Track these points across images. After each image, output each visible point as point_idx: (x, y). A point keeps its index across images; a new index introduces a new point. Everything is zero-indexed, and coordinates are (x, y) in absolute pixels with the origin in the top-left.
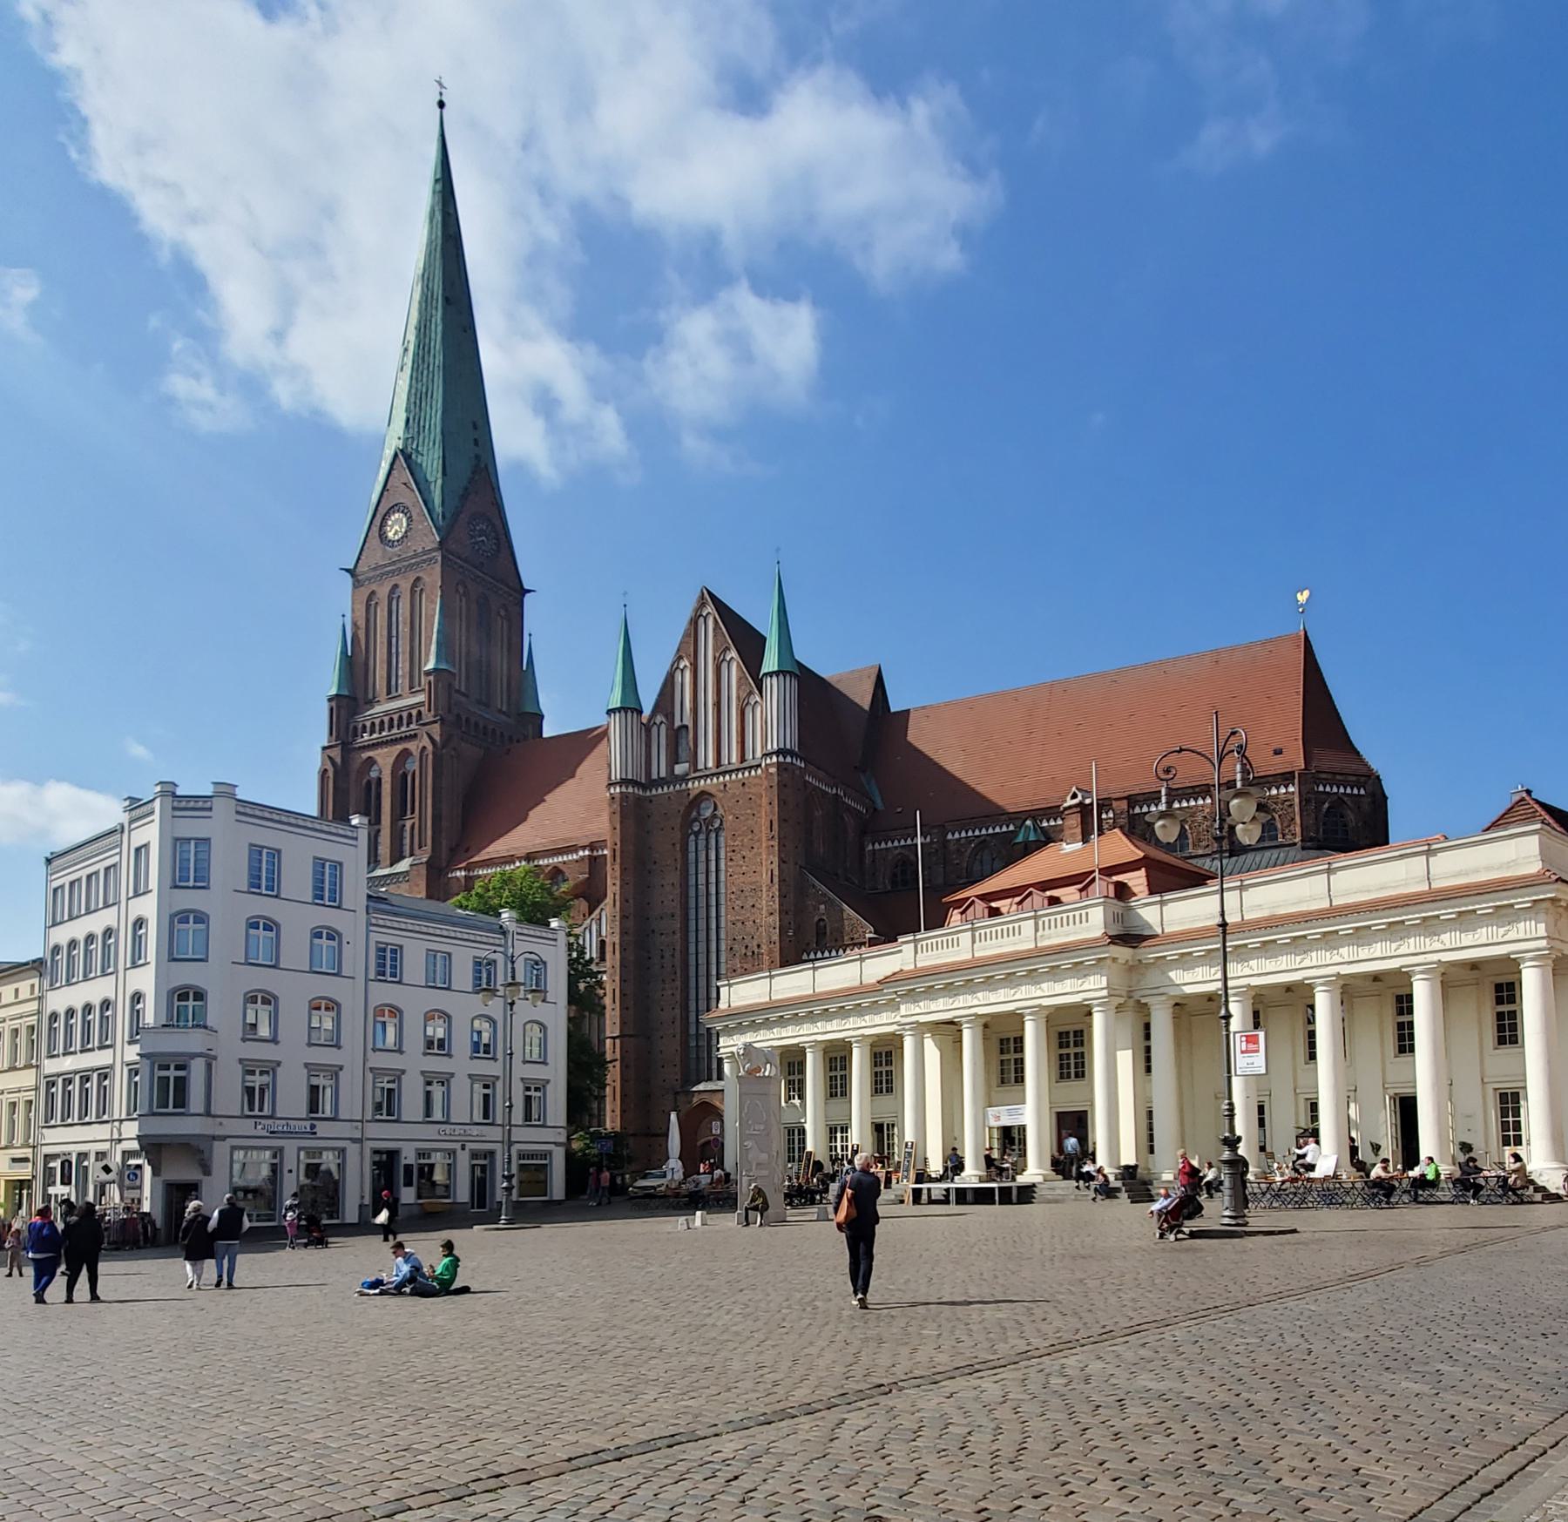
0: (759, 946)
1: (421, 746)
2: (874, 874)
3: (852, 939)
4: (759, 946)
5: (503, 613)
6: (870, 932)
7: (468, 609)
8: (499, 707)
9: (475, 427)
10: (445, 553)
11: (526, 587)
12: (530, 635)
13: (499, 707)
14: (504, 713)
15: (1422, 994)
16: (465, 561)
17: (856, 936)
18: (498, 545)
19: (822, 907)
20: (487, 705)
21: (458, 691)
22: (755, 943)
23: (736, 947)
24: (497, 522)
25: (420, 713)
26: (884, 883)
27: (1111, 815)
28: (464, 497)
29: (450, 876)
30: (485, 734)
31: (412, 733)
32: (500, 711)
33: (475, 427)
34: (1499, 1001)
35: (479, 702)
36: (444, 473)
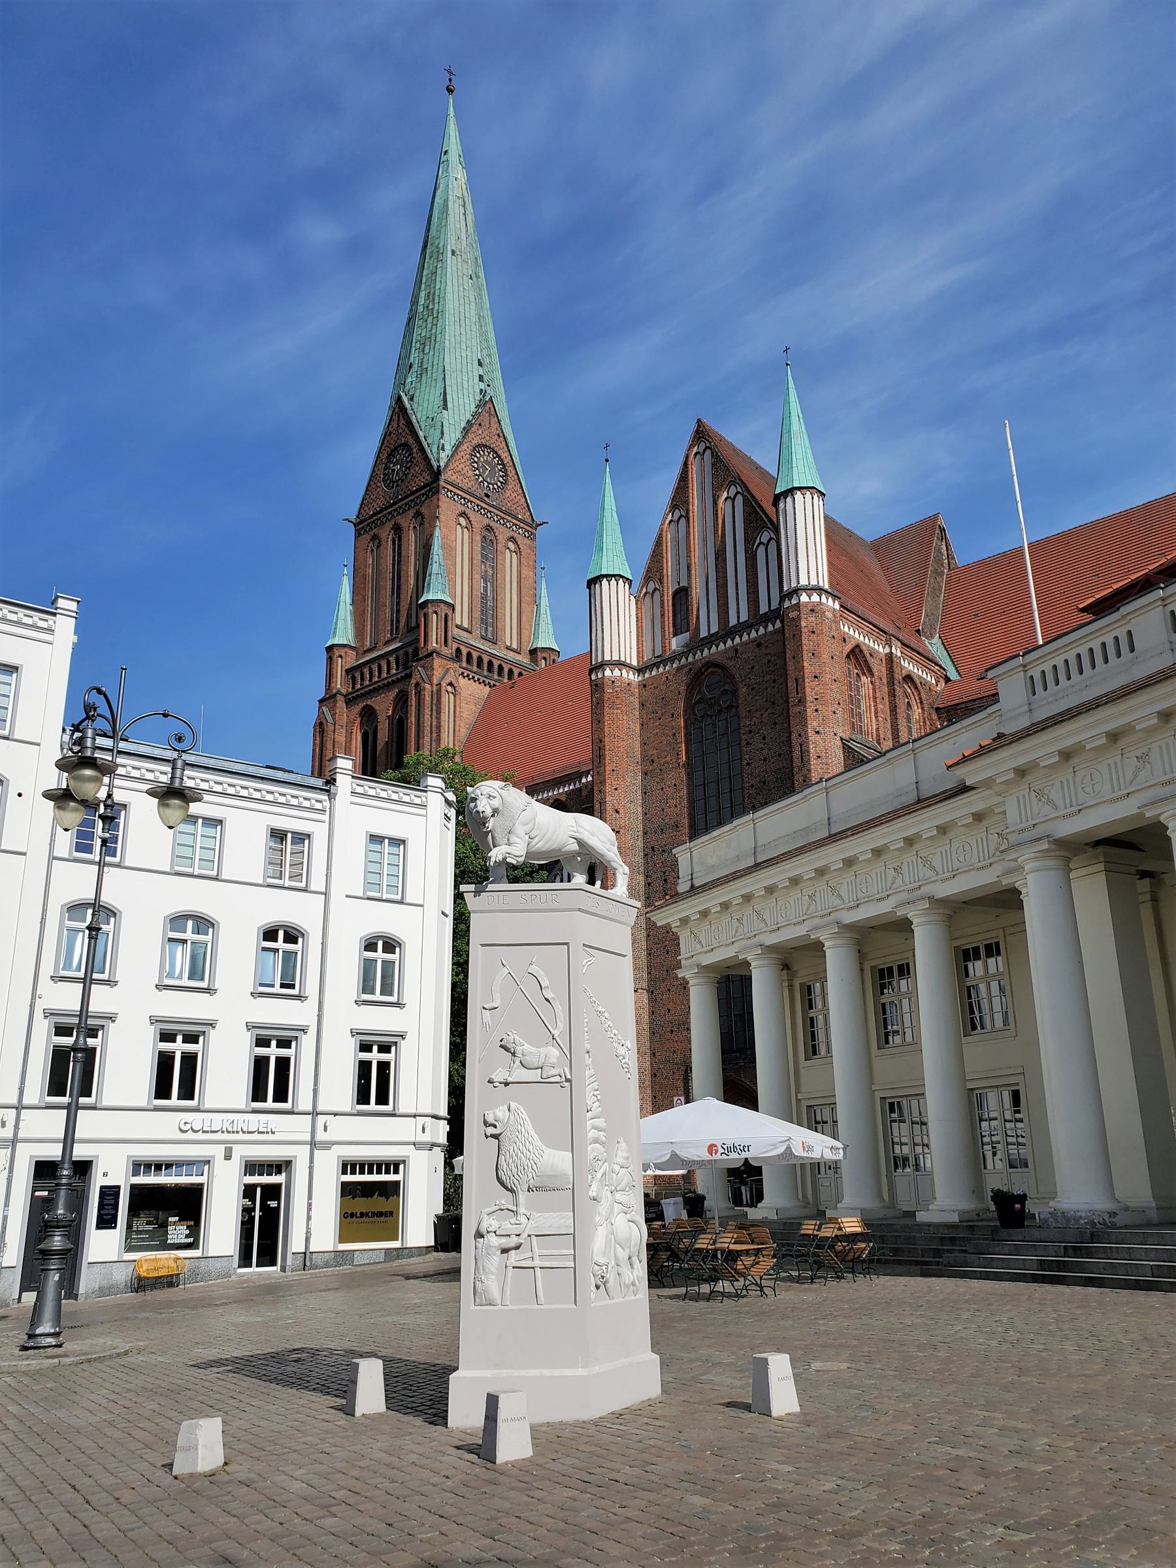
28: (466, 431)
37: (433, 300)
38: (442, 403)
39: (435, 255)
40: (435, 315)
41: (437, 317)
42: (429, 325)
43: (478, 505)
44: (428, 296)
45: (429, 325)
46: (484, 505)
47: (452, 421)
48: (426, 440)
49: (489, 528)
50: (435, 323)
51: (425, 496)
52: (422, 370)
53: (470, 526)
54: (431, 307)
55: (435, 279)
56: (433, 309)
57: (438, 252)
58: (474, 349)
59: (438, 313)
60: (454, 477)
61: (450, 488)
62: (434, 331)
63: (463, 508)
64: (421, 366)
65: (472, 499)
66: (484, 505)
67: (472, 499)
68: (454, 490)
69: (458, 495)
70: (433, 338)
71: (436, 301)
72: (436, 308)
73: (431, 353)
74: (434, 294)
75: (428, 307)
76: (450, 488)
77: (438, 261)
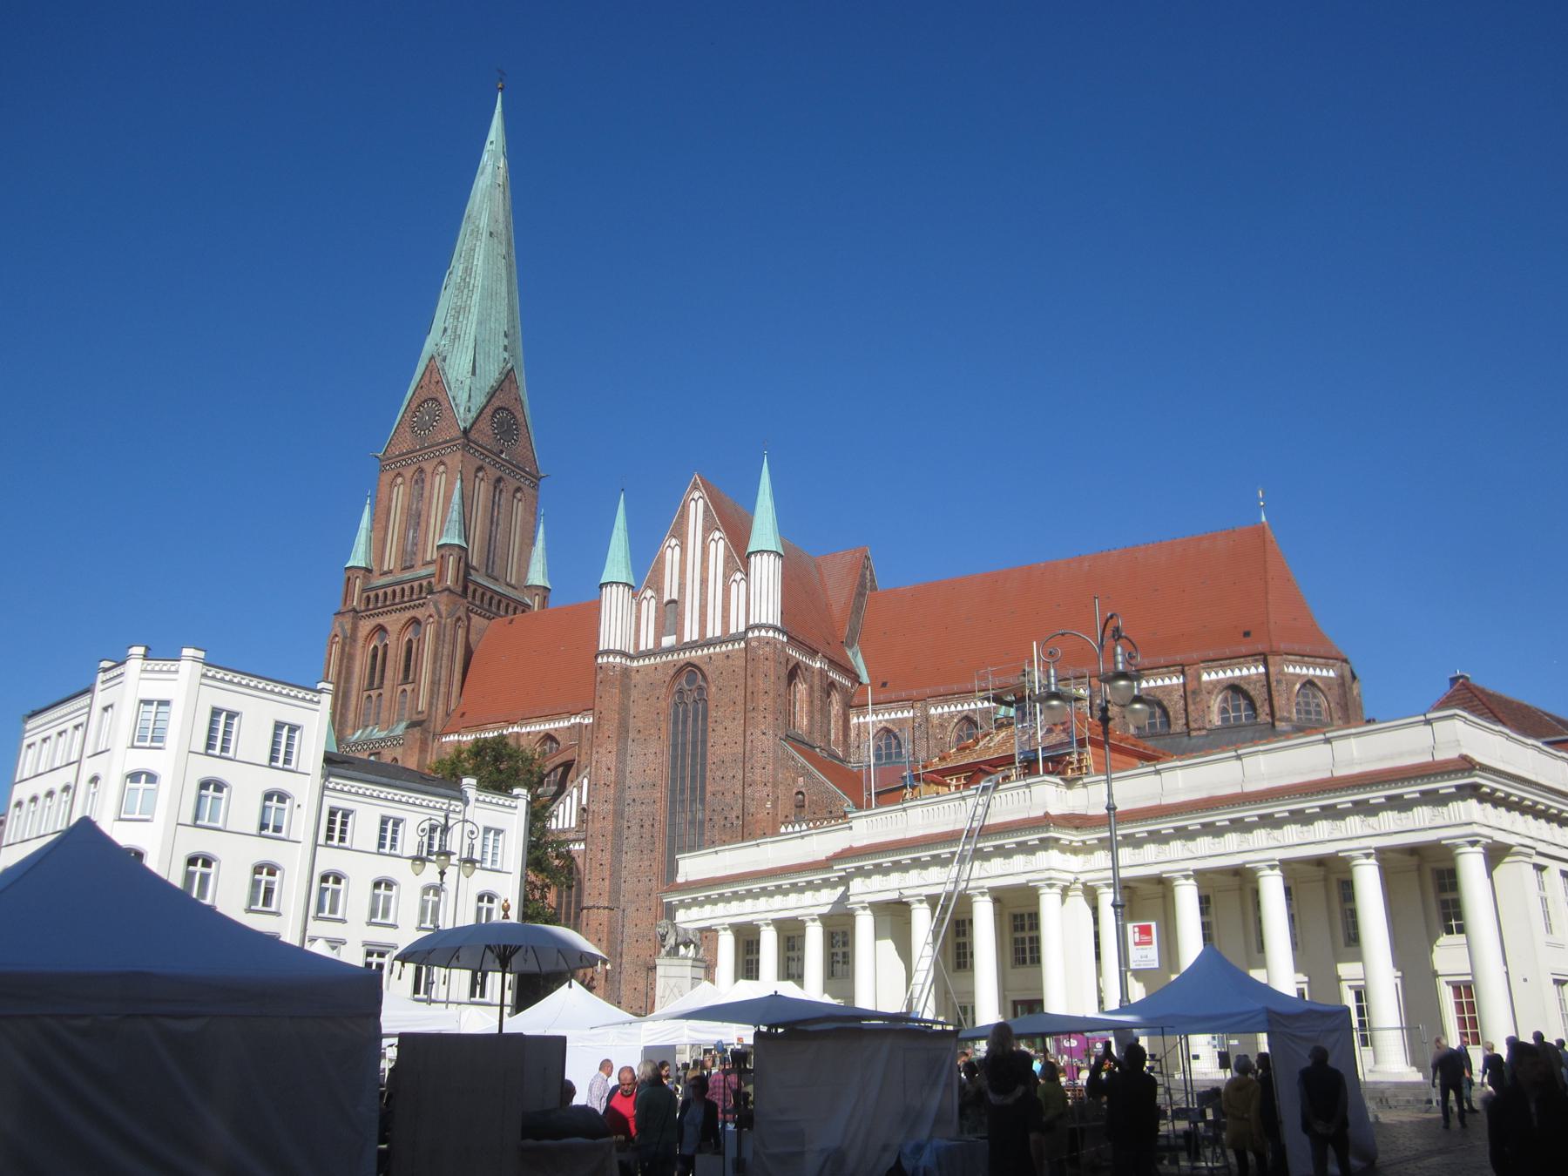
29: (444, 740)
36: (474, 373)
37: (471, 274)
38: (471, 369)
39: (475, 234)
40: (471, 288)
41: (473, 290)
42: (465, 297)
44: (466, 270)
45: (465, 297)
47: (478, 386)
48: (454, 400)
50: (470, 295)
52: (456, 335)
54: (467, 280)
55: (474, 256)
56: (469, 283)
57: (478, 231)
59: (474, 286)
62: (468, 302)
64: (455, 332)
70: (467, 309)
71: (473, 275)
72: (472, 282)
73: (465, 322)
74: (472, 269)
75: (465, 279)
77: (477, 240)
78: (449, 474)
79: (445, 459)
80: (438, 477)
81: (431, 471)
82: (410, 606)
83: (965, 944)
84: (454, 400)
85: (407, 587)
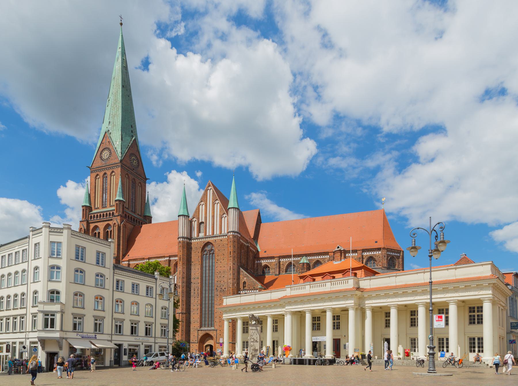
0: (225, 288)
1: (114, 223)
2: (257, 270)
3: (254, 288)
4: (225, 288)
5: (140, 185)
6: (260, 286)
7: (129, 183)
8: (138, 213)
9: (132, 127)
10: (122, 165)
11: (147, 177)
12: (148, 192)
13: (138, 213)
14: (139, 215)
15: (393, 313)
16: (129, 168)
17: (255, 287)
18: (138, 163)
19: (245, 278)
20: (135, 213)
21: (126, 207)
22: (224, 288)
23: (218, 288)
24: (138, 157)
25: (113, 213)
26: (260, 272)
27: (328, 257)
30: (134, 221)
31: (111, 219)
32: (138, 215)
33: (132, 127)
34: (412, 315)
35: (132, 211)
43: (131, 172)
46: (133, 172)
48: (116, 149)
49: (134, 179)
51: (116, 167)
53: (129, 178)
58: (130, 121)
60: (125, 163)
61: (124, 166)
63: (127, 172)
65: (130, 170)
66: (133, 172)
67: (130, 170)
68: (125, 167)
69: (126, 168)
76: (124, 166)
78: (116, 176)
79: (114, 170)
80: (112, 176)
81: (110, 174)
82: (104, 220)
83: (415, 319)
84: (116, 149)
85: (105, 213)
